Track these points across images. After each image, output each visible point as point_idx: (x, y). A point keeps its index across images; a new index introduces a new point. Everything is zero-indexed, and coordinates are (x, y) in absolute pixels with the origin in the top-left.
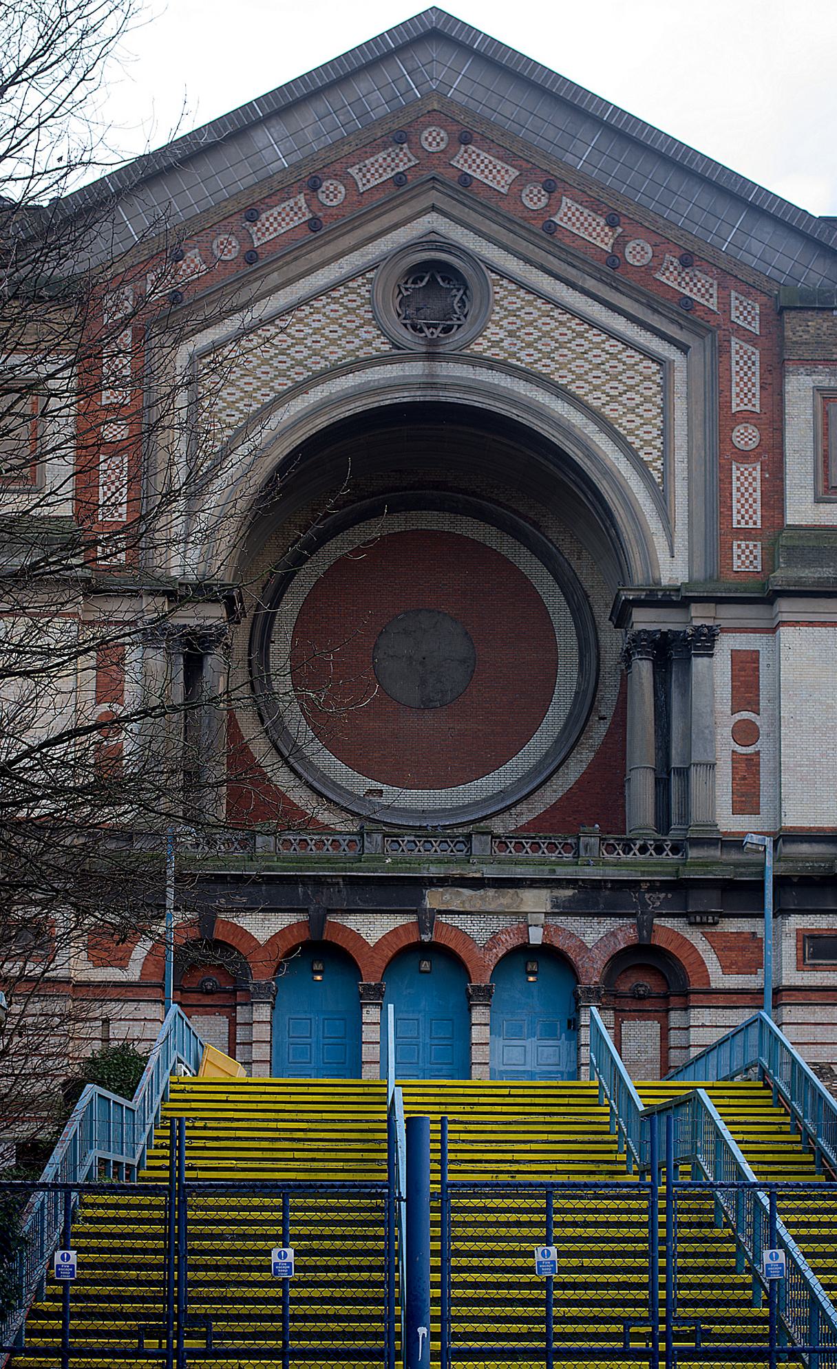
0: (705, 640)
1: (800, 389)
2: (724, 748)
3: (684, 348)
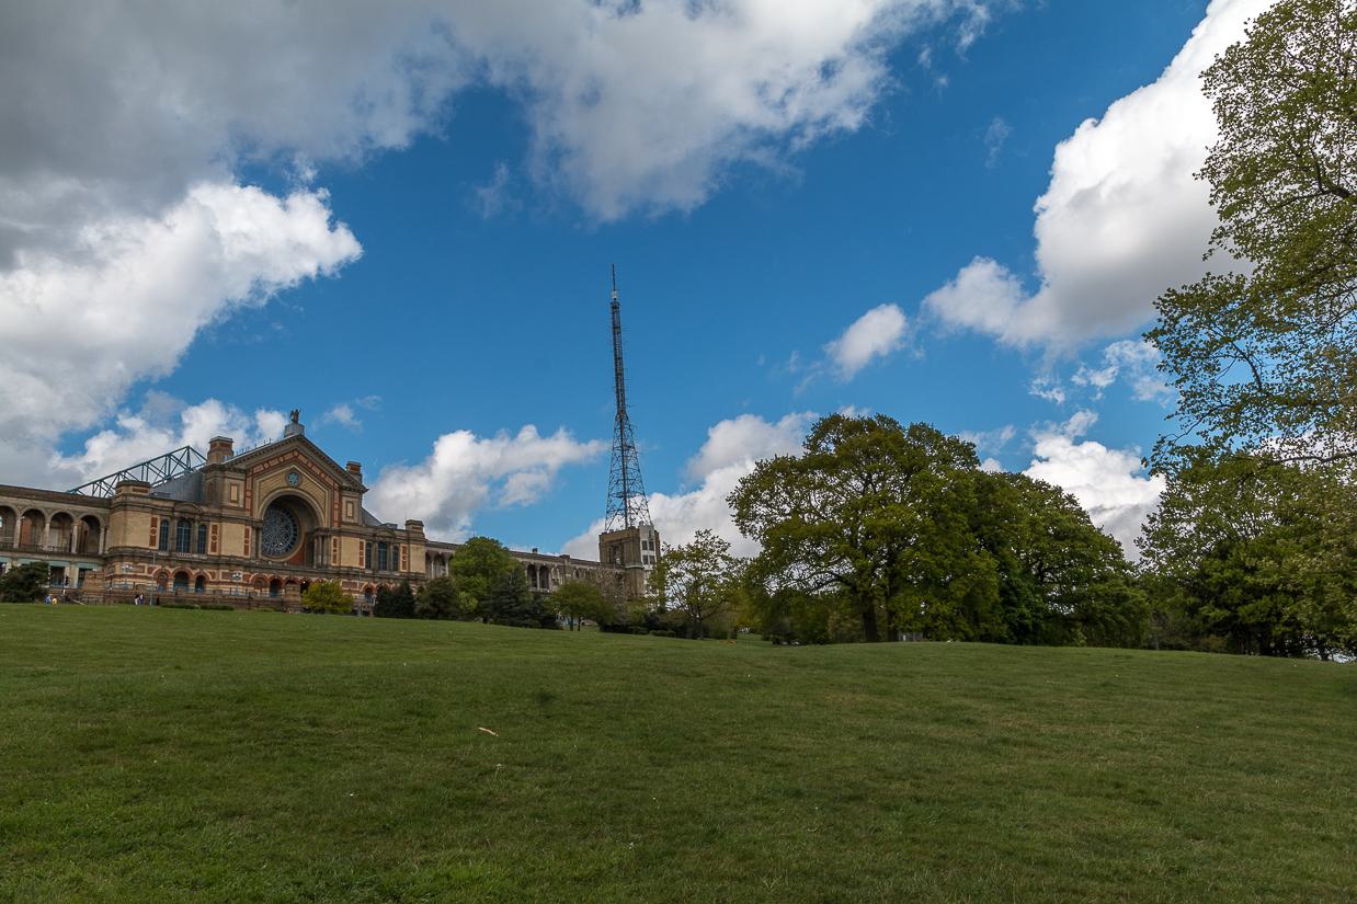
0: (330, 537)
1: (344, 499)
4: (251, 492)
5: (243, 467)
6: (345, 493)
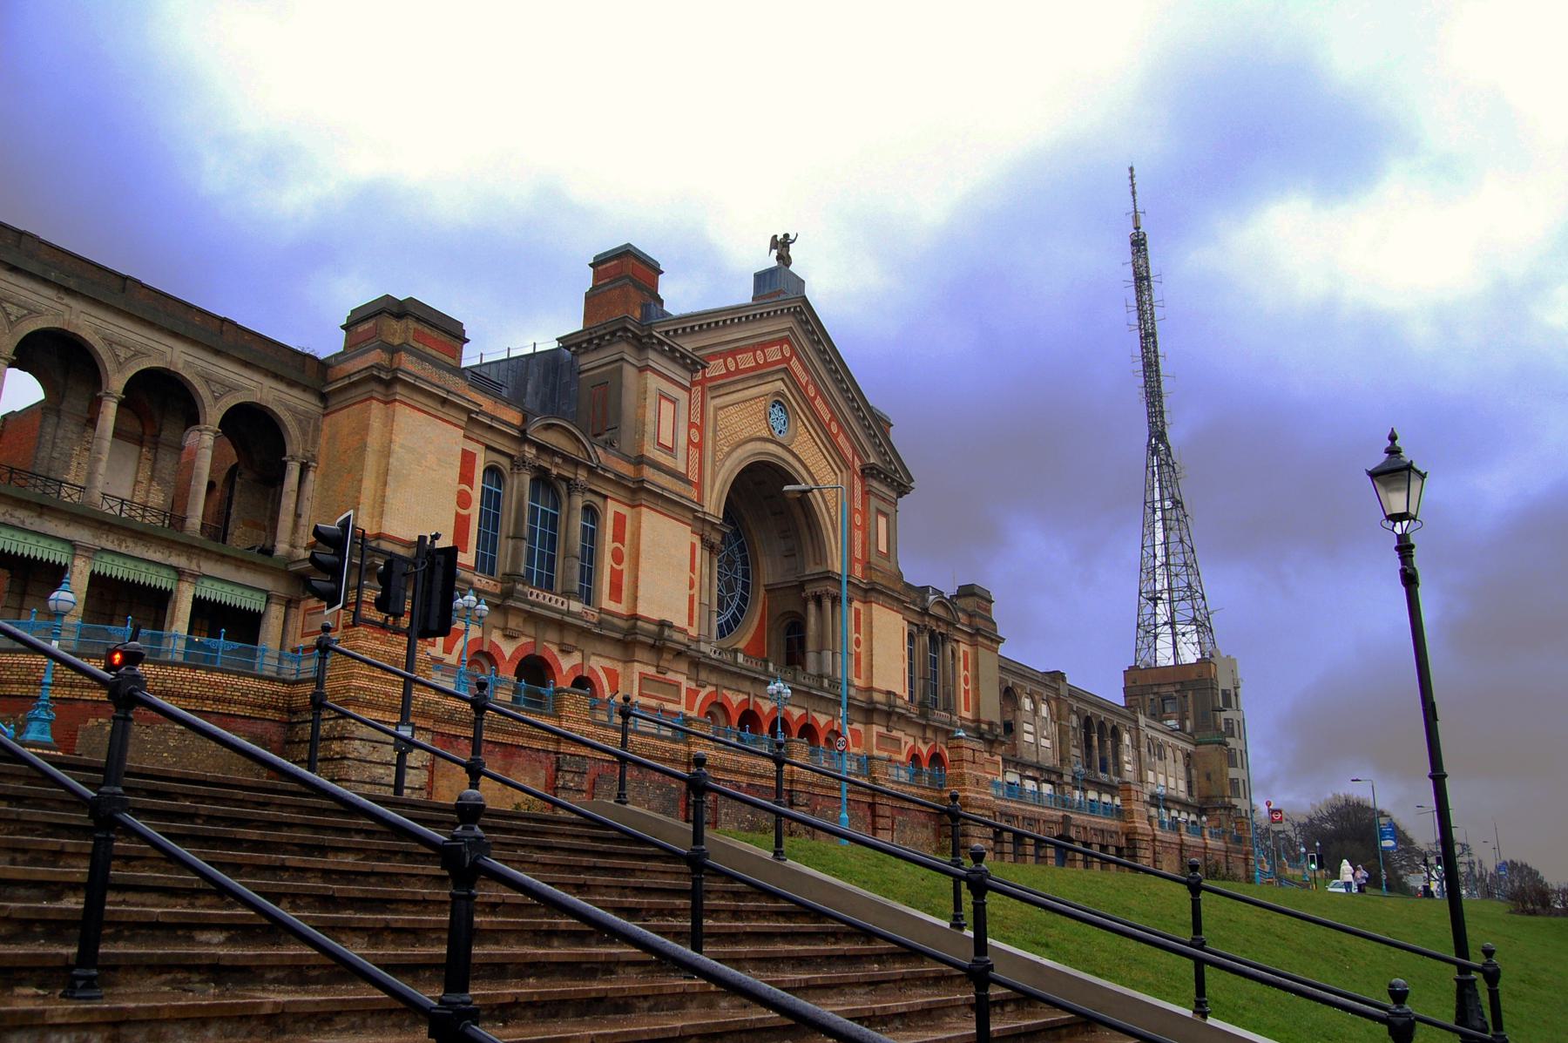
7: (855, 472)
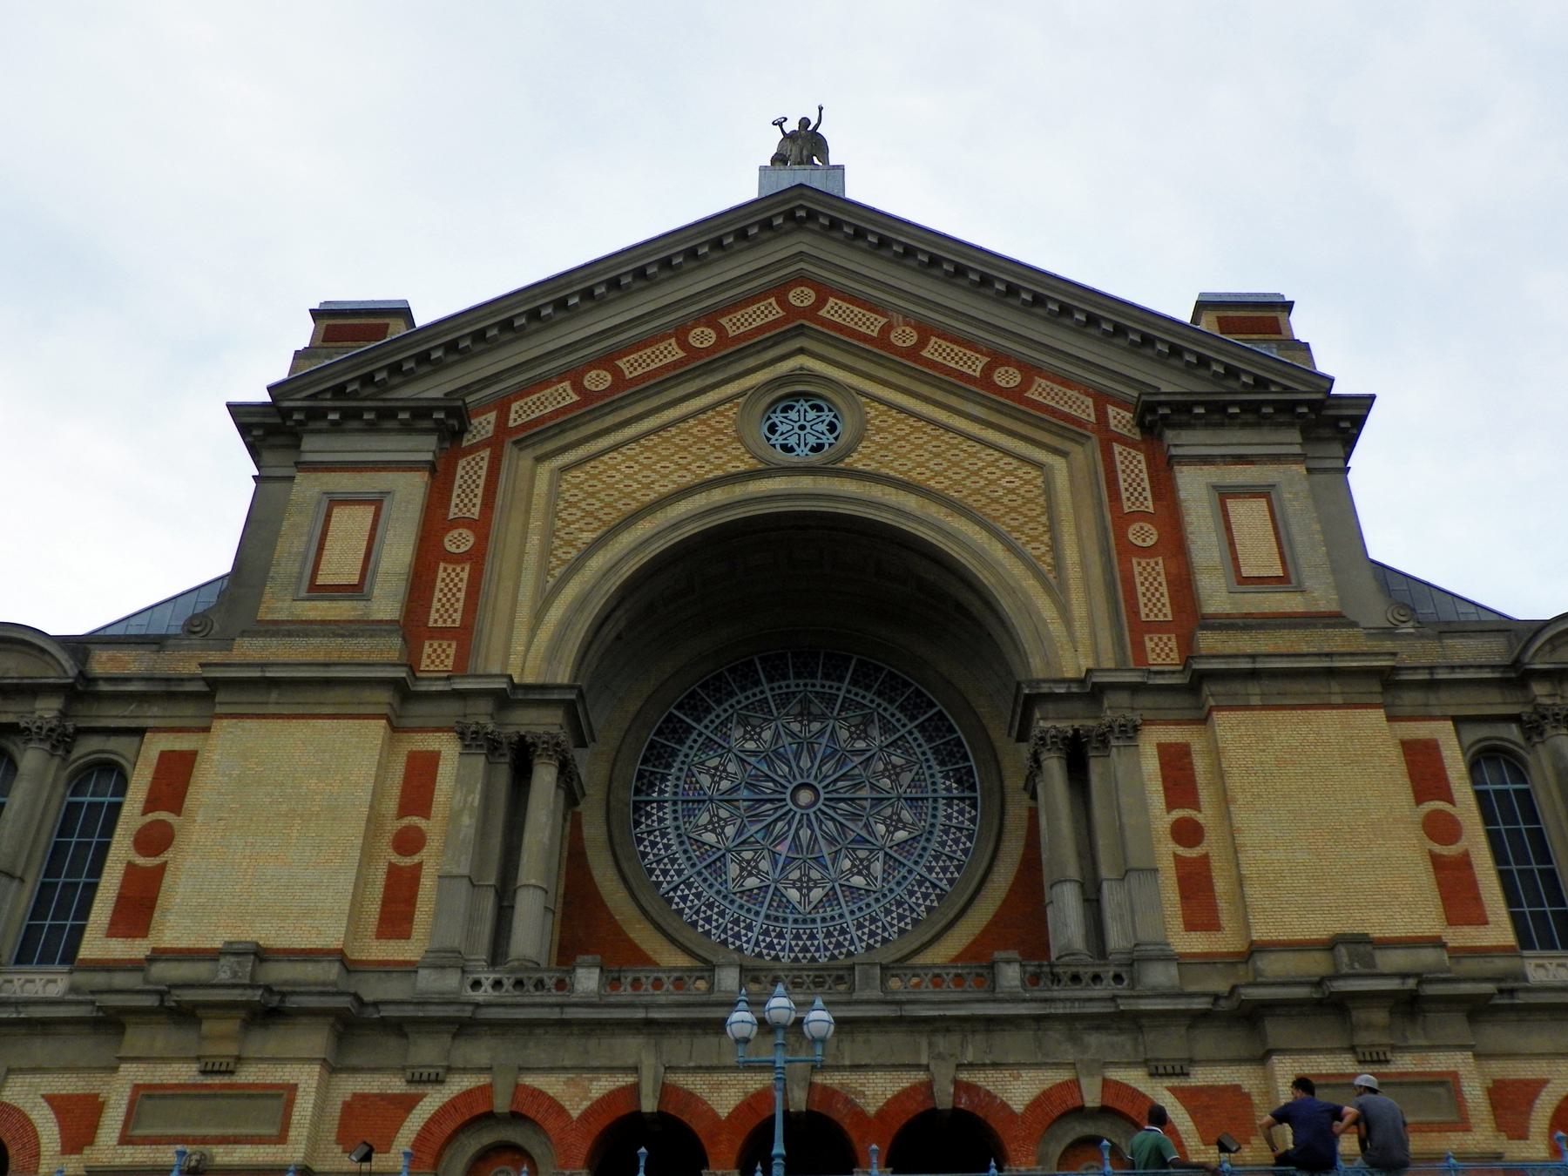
1: (1193, 484)
2: (1166, 851)
3: (1063, 454)
4: (481, 527)
5: (432, 389)
6: (1185, 441)
7: (1108, 439)
